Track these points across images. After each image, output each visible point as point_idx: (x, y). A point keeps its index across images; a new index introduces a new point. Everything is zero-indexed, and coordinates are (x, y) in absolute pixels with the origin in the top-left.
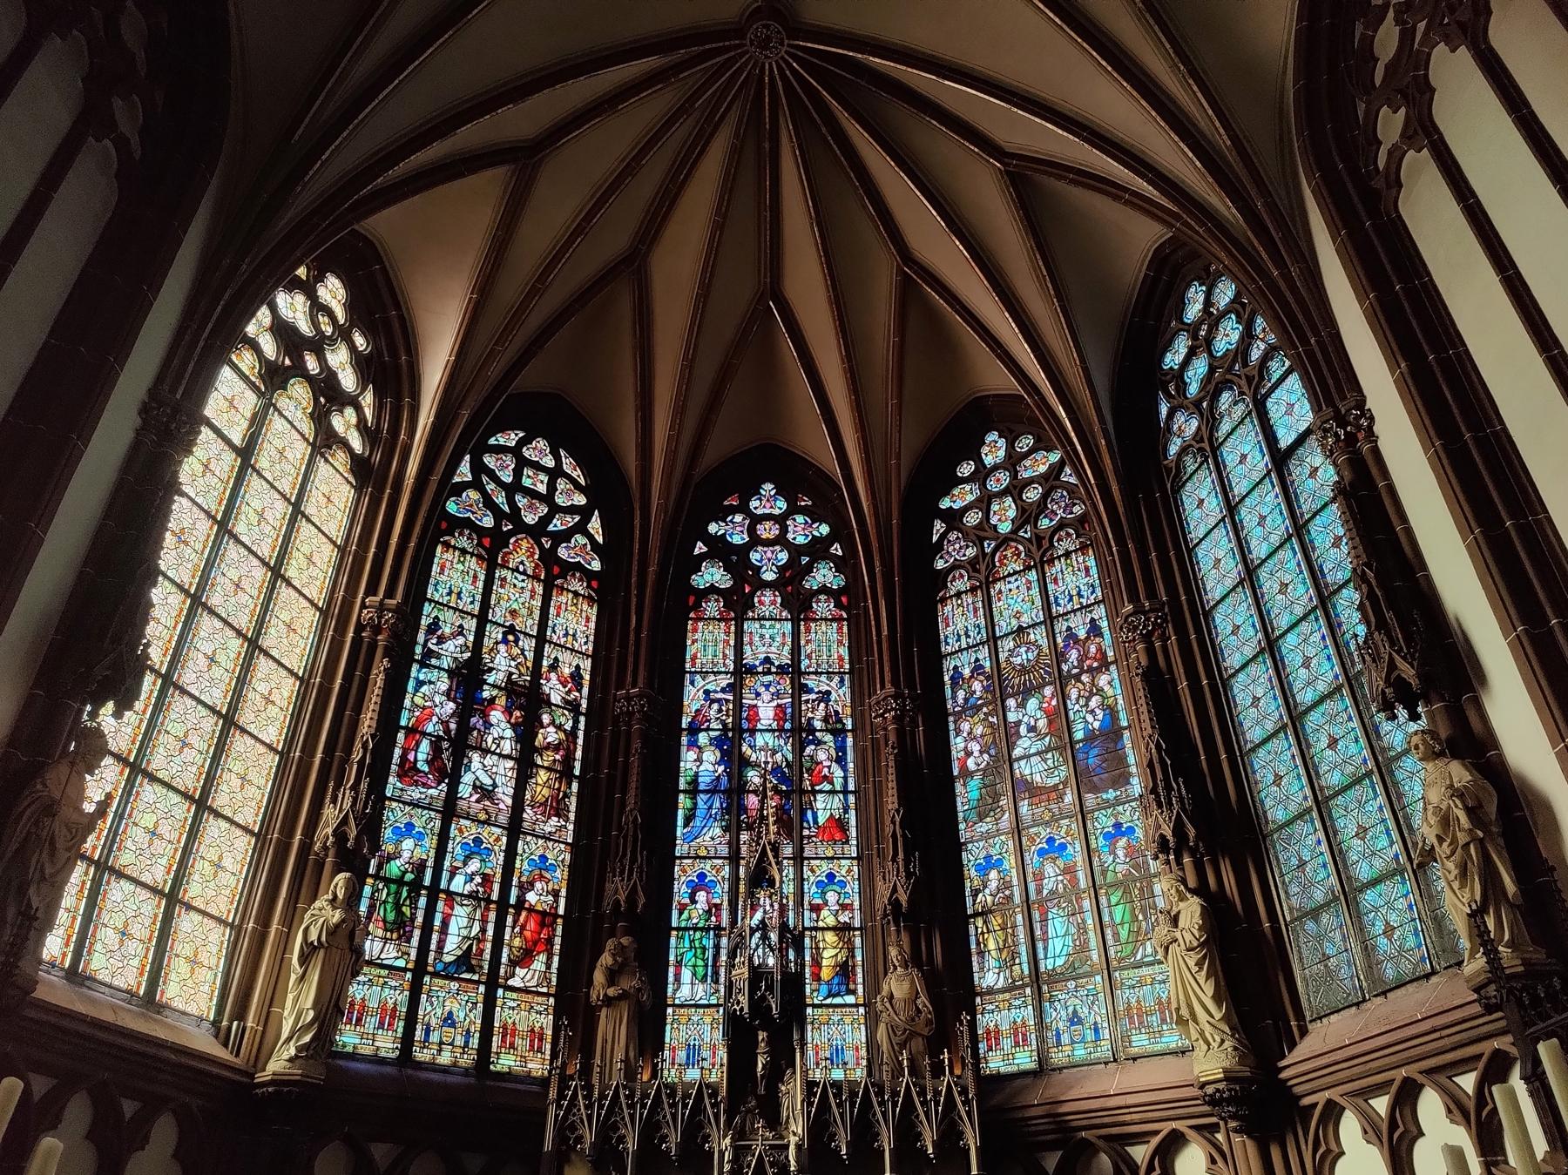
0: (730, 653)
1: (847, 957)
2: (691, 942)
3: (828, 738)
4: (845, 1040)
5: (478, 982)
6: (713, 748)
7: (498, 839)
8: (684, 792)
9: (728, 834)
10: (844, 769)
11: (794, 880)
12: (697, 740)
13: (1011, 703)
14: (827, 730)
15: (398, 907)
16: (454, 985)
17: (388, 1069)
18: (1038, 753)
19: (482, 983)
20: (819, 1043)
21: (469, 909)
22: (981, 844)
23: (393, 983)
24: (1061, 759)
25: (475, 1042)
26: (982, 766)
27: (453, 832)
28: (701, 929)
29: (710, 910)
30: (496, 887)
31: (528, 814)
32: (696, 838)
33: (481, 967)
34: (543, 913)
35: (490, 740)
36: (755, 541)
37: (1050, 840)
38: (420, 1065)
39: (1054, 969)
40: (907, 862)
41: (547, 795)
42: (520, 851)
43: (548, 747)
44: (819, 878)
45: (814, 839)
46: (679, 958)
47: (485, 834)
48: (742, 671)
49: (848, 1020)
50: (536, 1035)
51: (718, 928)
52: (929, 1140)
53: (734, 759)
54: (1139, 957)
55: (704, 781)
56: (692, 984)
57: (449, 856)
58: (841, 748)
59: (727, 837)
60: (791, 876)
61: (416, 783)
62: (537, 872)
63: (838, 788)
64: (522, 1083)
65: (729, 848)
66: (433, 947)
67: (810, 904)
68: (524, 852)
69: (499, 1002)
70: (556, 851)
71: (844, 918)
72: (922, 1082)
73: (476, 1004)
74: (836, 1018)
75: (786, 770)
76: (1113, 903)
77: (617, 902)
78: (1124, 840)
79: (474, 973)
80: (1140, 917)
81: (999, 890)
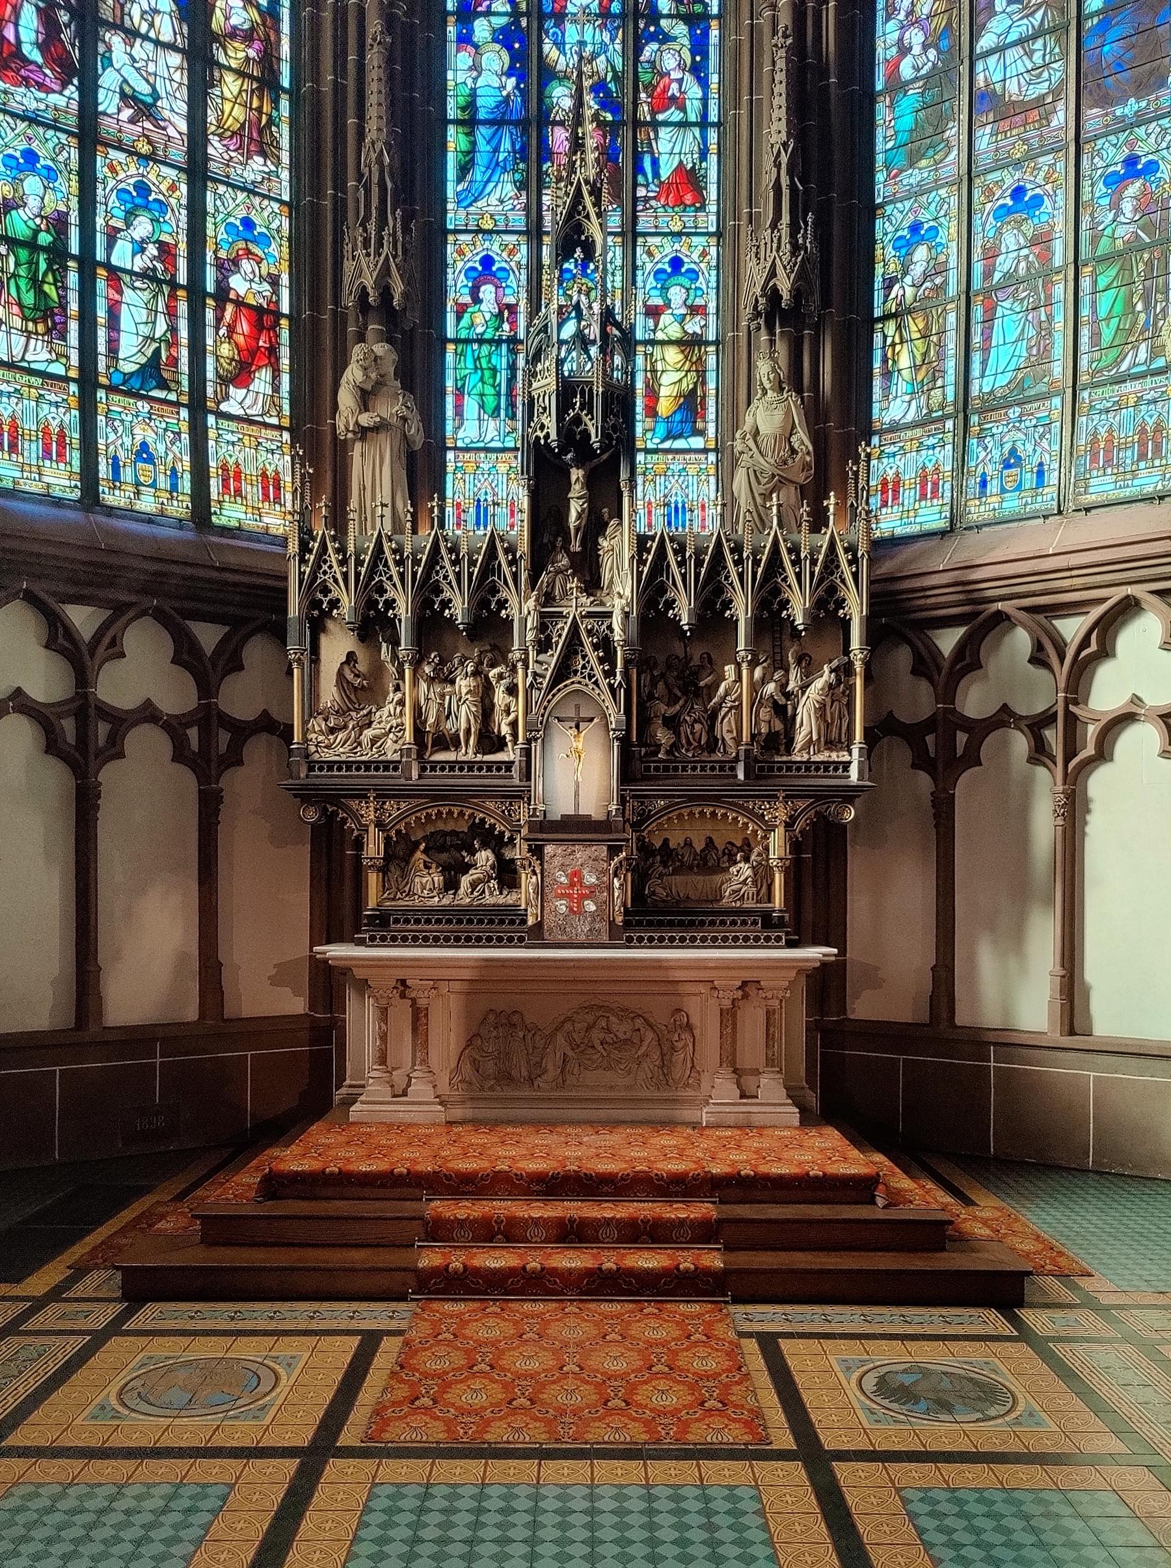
1: (695, 384)
2: (475, 361)
3: (680, 30)
4: (687, 496)
5: (177, 404)
6: (497, 47)
7: (173, 188)
8: (458, 122)
9: (524, 193)
10: (704, 83)
11: (622, 268)
12: (471, 32)
14: (678, 16)
15: (36, 284)
16: (143, 407)
17: (70, 515)
18: (1020, 42)
19: (183, 405)
20: (653, 500)
21: (146, 295)
22: (908, 204)
23: (53, 398)
24: (1057, 50)
25: (186, 484)
26: (923, 72)
27: (101, 170)
28: (490, 342)
29: (501, 313)
30: (182, 264)
31: (215, 148)
32: (476, 200)
33: (178, 383)
34: (258, 310)
35: (136, 12)
37: (1018, 192)
38: (110, 511)
39: (992, 391)
40: (794, 228)
41: (242, 119)
42: (210, 208)
43: (233, 33)
44: (660, 266)
45: (653, 203)
46: (460, 384)
47: (152, 177)
49: (692, 470)
50: (270, 485)
51: (513, 341)
52: (799, 608)
54: (1124, 367)
55: (486, 104)
56: (479, 419)
57: (100, 209)
58: (699, 46)
59: (523, 199)
60: (619, 262)
61: (26, 82)
62: (242, 245)
63: (692, 117)
64: (259, 541)
65: (527, 216)
66: (102, 348)
67: (645, 305)
68: (217, 210)
69: (212, 434)
70: (266, 214)
71: (693, 326)
72: (794, 537)
73: (179, 434)
74: (676, 467)
75: (612, 86)
76: (1101, 286)
77: (364, 293)
78: (1138, 184)
79: (170, 390)
80: (1139, 307)
81: (926, 276)
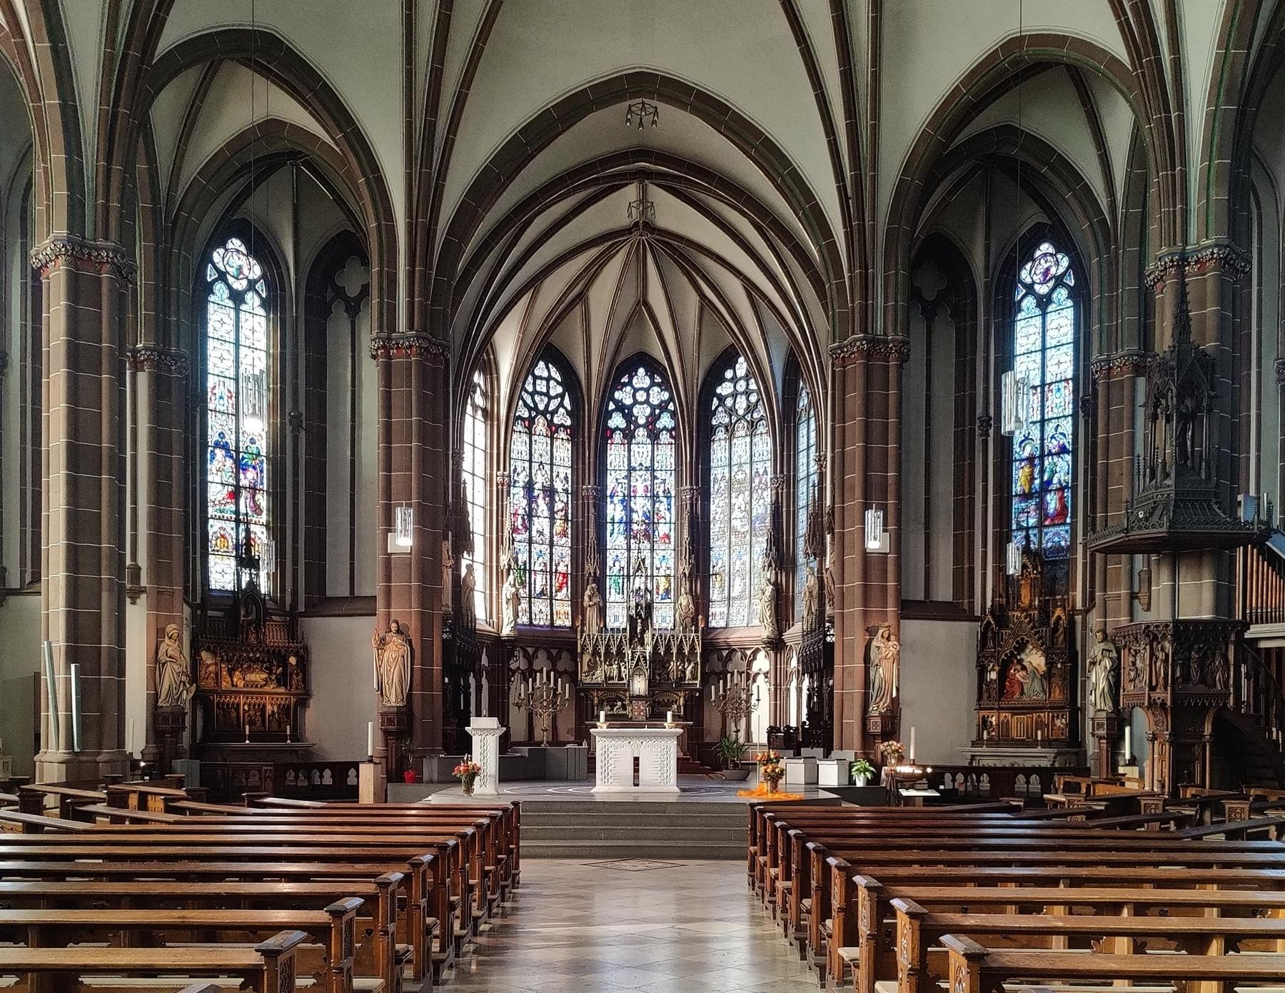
0: (626, 460)
13: (733, 495)
31: (555, 538)
36: (636, 402)
48: (631, 469)
53: (629, 510)
71: (668, 572)
